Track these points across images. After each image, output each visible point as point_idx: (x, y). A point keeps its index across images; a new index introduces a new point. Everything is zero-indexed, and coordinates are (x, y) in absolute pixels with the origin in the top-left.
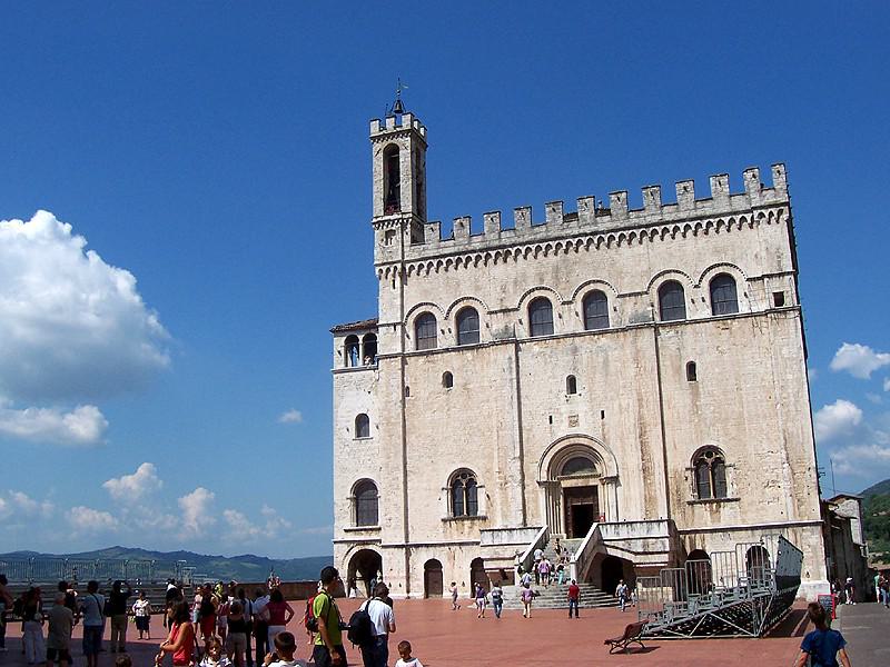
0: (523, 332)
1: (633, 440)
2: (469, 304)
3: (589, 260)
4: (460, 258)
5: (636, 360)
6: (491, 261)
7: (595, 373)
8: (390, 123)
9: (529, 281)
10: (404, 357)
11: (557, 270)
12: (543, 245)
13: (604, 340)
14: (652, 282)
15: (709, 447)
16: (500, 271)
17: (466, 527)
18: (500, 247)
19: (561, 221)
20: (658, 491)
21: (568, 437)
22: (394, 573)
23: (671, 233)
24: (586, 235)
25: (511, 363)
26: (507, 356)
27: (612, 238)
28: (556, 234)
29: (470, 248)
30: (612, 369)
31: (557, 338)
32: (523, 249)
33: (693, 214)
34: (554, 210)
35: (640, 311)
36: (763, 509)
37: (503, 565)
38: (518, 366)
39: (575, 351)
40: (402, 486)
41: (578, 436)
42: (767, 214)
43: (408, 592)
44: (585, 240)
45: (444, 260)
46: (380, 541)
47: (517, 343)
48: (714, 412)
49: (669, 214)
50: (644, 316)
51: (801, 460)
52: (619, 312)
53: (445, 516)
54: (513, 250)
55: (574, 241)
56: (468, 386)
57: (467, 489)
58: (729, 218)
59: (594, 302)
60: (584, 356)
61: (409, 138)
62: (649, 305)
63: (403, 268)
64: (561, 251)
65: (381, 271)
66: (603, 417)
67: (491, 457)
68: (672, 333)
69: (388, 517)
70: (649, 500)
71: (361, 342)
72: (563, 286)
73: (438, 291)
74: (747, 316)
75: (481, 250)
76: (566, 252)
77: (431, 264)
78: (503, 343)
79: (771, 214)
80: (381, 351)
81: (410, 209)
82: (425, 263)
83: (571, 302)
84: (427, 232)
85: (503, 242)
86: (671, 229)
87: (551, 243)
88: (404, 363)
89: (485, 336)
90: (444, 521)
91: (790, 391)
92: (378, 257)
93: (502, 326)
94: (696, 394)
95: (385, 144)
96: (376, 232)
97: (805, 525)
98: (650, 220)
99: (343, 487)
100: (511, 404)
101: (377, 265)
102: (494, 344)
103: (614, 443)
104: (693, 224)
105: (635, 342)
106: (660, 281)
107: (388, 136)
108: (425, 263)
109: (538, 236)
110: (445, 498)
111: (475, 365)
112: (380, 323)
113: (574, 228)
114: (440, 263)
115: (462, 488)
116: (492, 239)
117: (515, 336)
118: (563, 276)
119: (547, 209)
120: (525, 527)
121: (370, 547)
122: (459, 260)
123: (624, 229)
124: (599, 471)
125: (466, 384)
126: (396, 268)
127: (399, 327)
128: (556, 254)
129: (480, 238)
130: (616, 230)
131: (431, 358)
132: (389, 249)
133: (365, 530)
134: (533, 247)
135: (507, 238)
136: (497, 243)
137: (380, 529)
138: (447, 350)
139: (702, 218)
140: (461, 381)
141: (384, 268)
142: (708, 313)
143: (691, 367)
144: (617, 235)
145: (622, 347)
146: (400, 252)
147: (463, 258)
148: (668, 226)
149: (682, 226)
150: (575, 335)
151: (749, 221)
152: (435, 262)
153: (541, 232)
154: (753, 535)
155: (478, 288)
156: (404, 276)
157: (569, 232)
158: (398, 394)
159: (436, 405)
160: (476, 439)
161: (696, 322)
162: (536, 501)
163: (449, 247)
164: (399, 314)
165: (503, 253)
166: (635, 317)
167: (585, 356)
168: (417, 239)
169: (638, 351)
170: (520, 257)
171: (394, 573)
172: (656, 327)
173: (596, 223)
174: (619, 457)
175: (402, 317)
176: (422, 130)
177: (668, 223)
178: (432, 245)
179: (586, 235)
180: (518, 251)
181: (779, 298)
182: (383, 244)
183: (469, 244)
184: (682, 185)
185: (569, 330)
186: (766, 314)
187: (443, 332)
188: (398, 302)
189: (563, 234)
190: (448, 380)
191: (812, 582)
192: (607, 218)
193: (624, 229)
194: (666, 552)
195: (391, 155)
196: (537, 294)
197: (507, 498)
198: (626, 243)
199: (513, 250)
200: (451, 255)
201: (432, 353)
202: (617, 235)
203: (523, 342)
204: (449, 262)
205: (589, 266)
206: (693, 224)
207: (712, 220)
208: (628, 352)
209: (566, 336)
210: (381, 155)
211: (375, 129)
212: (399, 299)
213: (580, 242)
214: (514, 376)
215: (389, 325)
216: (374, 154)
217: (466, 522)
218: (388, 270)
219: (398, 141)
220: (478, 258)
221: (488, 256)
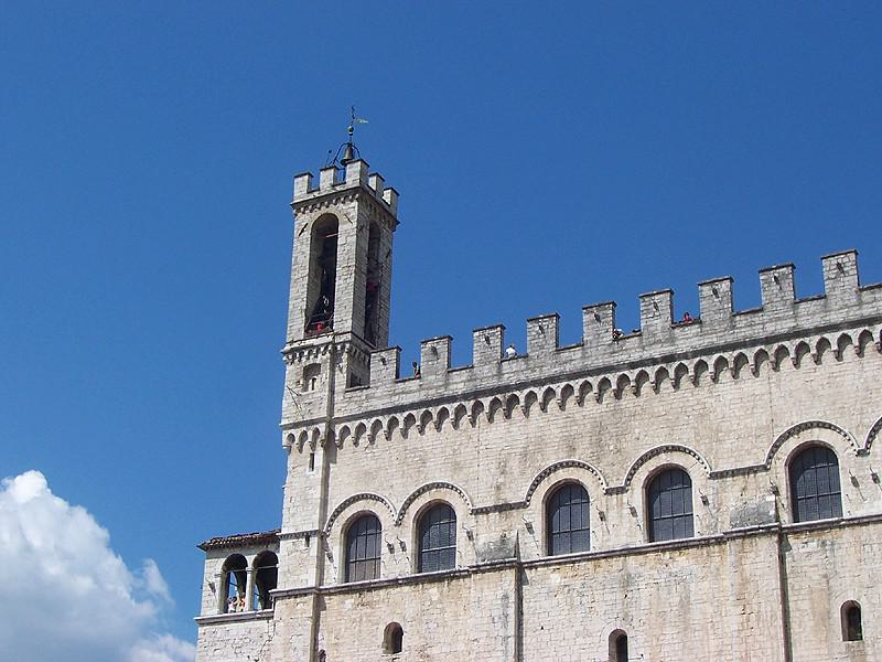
0: (533, 548)
3: (659, 408)
4: (431, 412)
6: (482, 417)
7: (662, 626)
8: (326, 179)
9: (549, 450)
10: (319, 595)
11: (599, 429)
12: (576, 384)
13: (683, 562)
14: (776, 447)
16: (501, 434)
18: (499, 390)
19: (609, 337)
23: (814, 351)
24: (654, 361)
26: (500, 593)
27: (702, 366)
28: (600, 363)
29: (447, 393)
30: (696, 616)
31: (595, 558)
32: (540, 392)
33: (854, 314)
34: (598, 318)
35: (752, 505)
38: (520, 613)
39: (627, 582)
44: (651, 371)
45: (401, 417)
47: (520, 568)
49: (810, 315)
50: (759, 513)
52: (713, 506)
54: (522, 395)
55: (632, 375)
56: (428, 652)
59: (667, 487)
60: (643, 594)
61: (355, 204)
62: (769, 493)
63: (330, 433)
64: (608, 395)
65: (292, 437)
68: (813, 545)
71: (250, 566)
72: (610, 459)
73: (385, 474)
75: (466, 396)
76: (618, 395)
77: (377, 425)
78: (494, 567)
80: (283, 584)
81: (348, 325)
82: (369, 423)
83: (621, 490)
84: (375, 365)
85: (505, 381)
87: (589, 379)
88: (319, 606)
89: (465, 557)
92: (289, 412)
93: (496, 537)
95: (316, 214)
96: (289, 368)
98: (771, 329)
101: (287, 427)
102: (478, 570)
104: (855, 334)
105: (739, 564)
106: (792, 444)
107: (321, 200)
108: (369, 423)
109: (568, 368)
111: (443, 611)
112: (283, 532)
113: (633, 351)
114: (393, 423)
116: (486, 376)
117: (517, 554)
118: (611, 440)
119: (586, 318)
122: (427, 417)
123: (726, 348)
126: (317, 432)
127: (314, 540)
128: (599, 400)
129: (465, 375)
130: (709, 351)
131: (368, 596)
132: (302, 402)
134: (558, 387)
135: (513, 373)
136: (494, 383)
138: (395, 583)
141: (297, 433)
143: (852, 614)
144: (711, 360)
145: (718, 573)
146: (325, 403)
147: (434, 411)
148: (807, 340)
149: (833, 337)
150: (628, 552)
152: (385, 421)
153: (574, 360)
155: (457, 467)
156: (331, 445)
157: (623, 358)
163: (412, 392)
165: (505, 400)
166: (742, 516)
167: (644, 593)
168: (357, 381)
169: (745, 582)
170: (535, 408)
172: (782, 535)
173: (672, 340)
176: (387, 196)
177: (807, 333)
178: (383, 389)
179: (654, 361)
180: (532, 396)
182: (298, 390)
183: (446, 385)
184: (834, 261)
185: (617, 543)
187: (391, 549)
188: (317, 493)
189: (612, 361)
190: (395, 638)
192: (695, 329)
193: (726, 348)
195: (325, 234)
196: (562, 475)
198: (728, 374)
200: (413, 406)
201: (370, 588)
202: (711, 360)
203: (532, 566)
204: (410, 420)
205: (659, 421)
206: (855, 334)
208: (727, 583)
209: (609, 555)
210: (307, 234)
211: (300, 189)
213: (643, 376)
214: (512, 631)
215: (297, 536)
216: (296, 233)
220: (460, 411)
221: (478, 407)
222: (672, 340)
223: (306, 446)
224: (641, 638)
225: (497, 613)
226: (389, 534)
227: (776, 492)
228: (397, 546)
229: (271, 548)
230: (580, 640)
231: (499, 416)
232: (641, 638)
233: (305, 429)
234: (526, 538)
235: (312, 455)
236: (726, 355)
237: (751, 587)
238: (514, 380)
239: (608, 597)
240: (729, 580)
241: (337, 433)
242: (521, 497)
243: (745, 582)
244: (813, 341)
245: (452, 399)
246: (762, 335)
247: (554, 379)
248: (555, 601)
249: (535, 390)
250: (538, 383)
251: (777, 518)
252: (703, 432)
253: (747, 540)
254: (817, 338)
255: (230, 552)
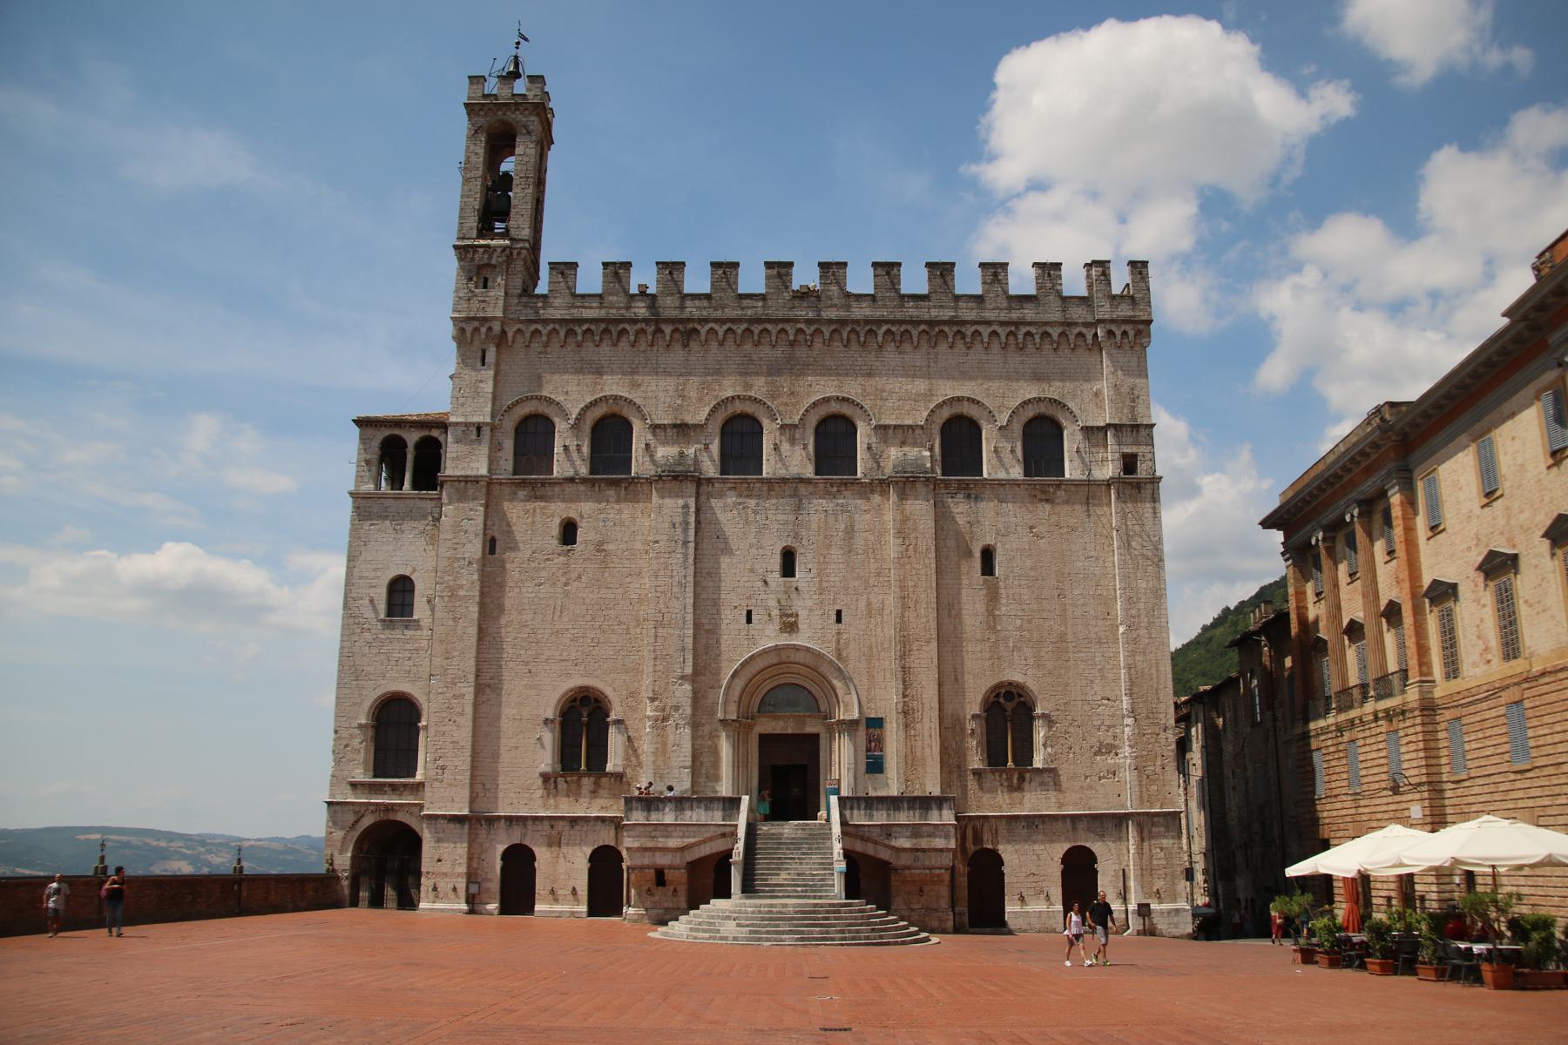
1: (889, 662)
2: (615, 409)
5: (901, 533)
7: (829, 547)
12: (757, 329)
15: (1010, 684)
17: (585, 790)
18: (681, 321)
20: (927, 750)
21: (777, 649)
22: (445, 867)
25: (686, 514)
28: (780, 315)
29: (628, 315)
30: (859, 542)
31: (769, 481)
32: (721, 330)
33: (1004, 316)
34: (779, 275)
36: (1090, 787)
37: (662, 860)
40: (469, 710)
41: (796, 648)
42: (1118, 333)
43: (467, 902)
46: (421, 807)
47: (699, 482)
48: (1020, 629)
51: (1152, 713)
53: (548, 769)
57: (588, 725)
58: (1060, 330)
66: (839, 620)
67: (636, 671)
69: (440, 763)
70: (911, 761)
74: (1075, 484)
75: (645, 320)
76: (792, 344)
79: (1125, 333)
81: (526, 233)
83: (795, 426)
86: (969, 333)
87: (769, 327)
89: (639, 464)
90: (546, 777)
91: (1142, 606)
94: (993, 597)
97: (1157, 814)
98: (934, 313)
99: (354, 704)
100: (683, 586)
103: (855, 666)
106: (946, 413)
110: (549, 738)
111: (620, 512)
112: (453, 419)
114: (570, 333)
115: (583, 724)
120: (695, 799)
121: (401, 817)
124: (822, 708)
125: (602, 543)
133: (391, 785)
136: (674, 313)
137: (420, 786)
139: (1017, 324)
140: (592, 536)
142: (1017, 472)
146: (501, 303)
151: (1089, 337)
154: (1074, 829)
158: (475, 548)
159: (544, 574)
160: (614, 638)
161: (1001, 484)
162: (715, 752)
164: (488, 409)
166: (901, 467)
167: (814, 518)
171: (445, 867)
174: (866, 689)
175: (493, 417)
179: (830, 321)
181: (1129, 463)
182: (471, 285)
183: (628, 308)
186: (1108, 484)
187: (566, 448)
188: (488, 387)
189: (792, 314)
190: (569, 532)
191: (1166, 906)
194: (949, 850)
197: (665, 744)
199: (703, 330)
201: (543, 484)
203: (710, 480)
207: (1033, 330)
209: (784, 481)
212: (491, 383)
214: (692, 538)
215: (467, 425)
217: (585, 781)
218: (476, 330)
219: (517, 117)
222: (848, 308)
223: (476, 343)
224: (810, 557)
225: (678, 519)
226: (562, 437)
227: (931, 450)
228: (573, 448)
229: (435, 433)
230: (753, 551)
231: (677, 347)
232: (810, 557)
233: (476, 324)
234: (704, 458)
235: (484, 352)
236: (894, 329)
237: (910, 524)
238: (696, 314)
239: (781, 517)
240: (890, 516)
241: (510, 335)
242: (701, 417)
243: (905, 520)
244: (969, 330)
245: (634, 321)
246: (927, 317)
247: (733, 321)
248: (730, 515)
249: (716, 327)
250: (722, 321)
251: (933, 470)
252: (869, 389)
253: (908, 485)
254: (974, 328)
255: (386, 432)
